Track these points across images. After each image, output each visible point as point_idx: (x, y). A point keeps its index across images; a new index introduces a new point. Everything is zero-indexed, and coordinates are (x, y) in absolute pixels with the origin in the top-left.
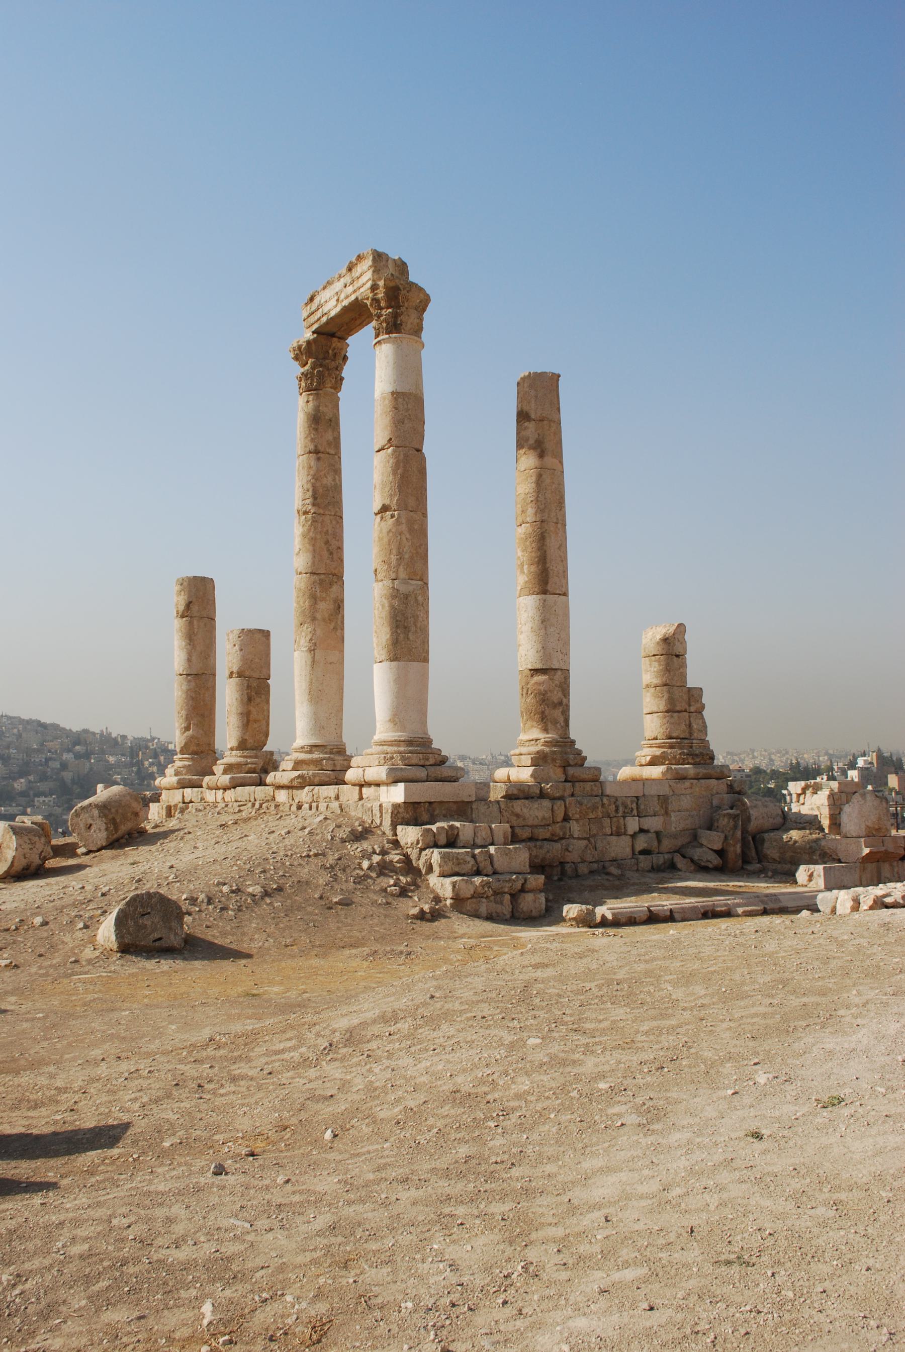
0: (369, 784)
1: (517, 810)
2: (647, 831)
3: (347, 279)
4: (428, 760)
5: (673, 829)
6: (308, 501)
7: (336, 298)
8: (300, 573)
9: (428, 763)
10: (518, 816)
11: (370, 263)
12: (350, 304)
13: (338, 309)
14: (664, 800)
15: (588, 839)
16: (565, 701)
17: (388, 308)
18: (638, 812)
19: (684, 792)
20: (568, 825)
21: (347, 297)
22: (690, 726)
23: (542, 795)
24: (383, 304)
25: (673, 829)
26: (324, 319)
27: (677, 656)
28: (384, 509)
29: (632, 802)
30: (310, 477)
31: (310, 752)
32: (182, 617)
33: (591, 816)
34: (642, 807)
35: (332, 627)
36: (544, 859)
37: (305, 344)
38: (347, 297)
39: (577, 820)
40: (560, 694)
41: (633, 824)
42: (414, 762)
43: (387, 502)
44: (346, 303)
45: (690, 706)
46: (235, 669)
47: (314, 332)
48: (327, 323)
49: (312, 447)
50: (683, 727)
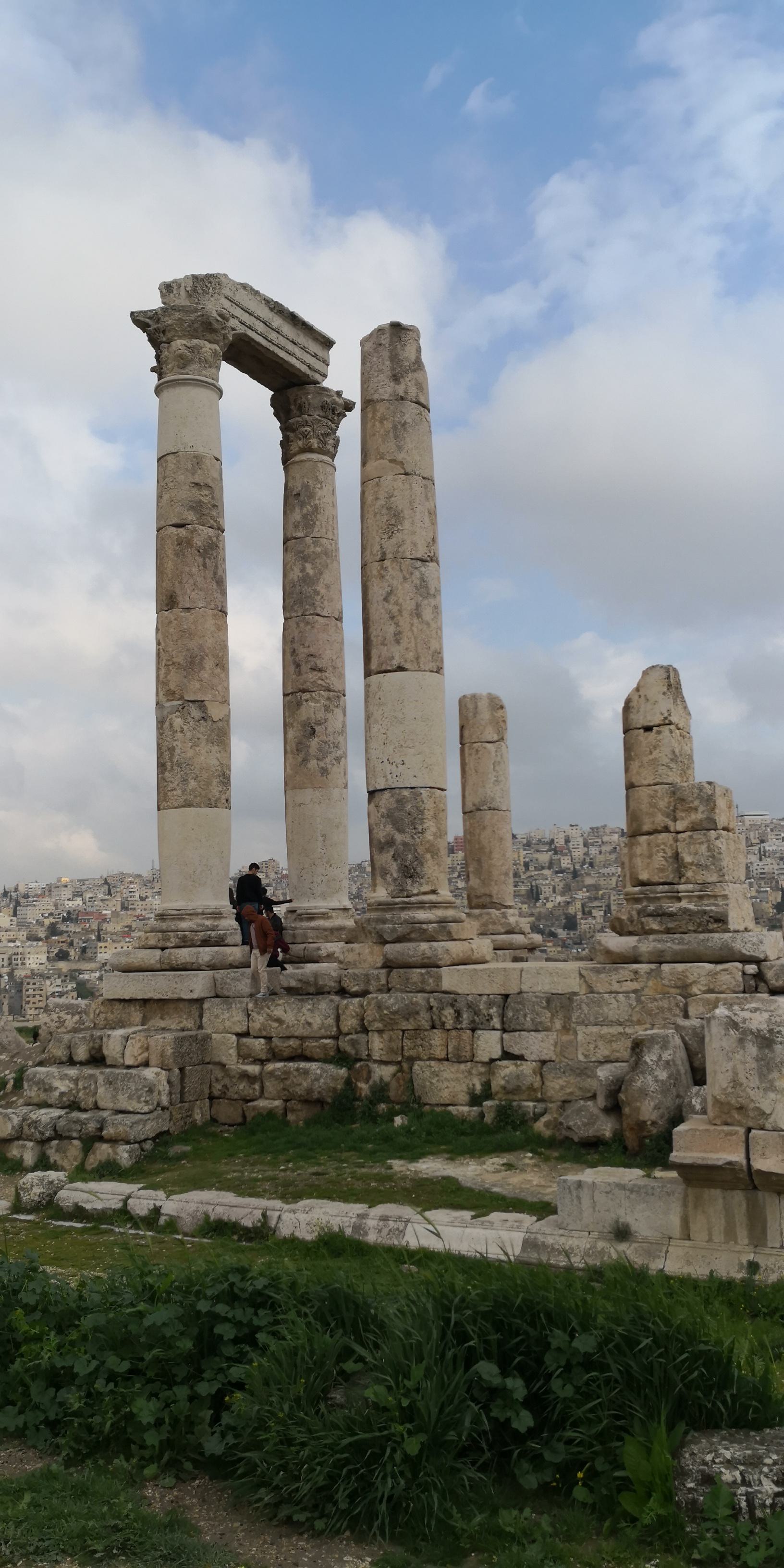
1: (278, 1012)
2: (521, 1058)
4: (169, 939)
5: (581, 1058)
10: (279, 1021)
14: (561, 1003)
15: (399, 1063)
16: (399, 837)
18: (503, 1023)
19: (616, 987)
20: (362, 1037)
22: (677, 856)
23: (342, 992)
25: (581, 1058)
27: (648, 729)
29: (490, 1004)
33: (405, 1025)
34: (510, 1014)
35: (300, 759)
36: (309, 1091)
39: (380, 1032)
40: (389, 828)
41: (489, 1043)
42: (152, 942)
45: (675, 820)
50: (659, 860)
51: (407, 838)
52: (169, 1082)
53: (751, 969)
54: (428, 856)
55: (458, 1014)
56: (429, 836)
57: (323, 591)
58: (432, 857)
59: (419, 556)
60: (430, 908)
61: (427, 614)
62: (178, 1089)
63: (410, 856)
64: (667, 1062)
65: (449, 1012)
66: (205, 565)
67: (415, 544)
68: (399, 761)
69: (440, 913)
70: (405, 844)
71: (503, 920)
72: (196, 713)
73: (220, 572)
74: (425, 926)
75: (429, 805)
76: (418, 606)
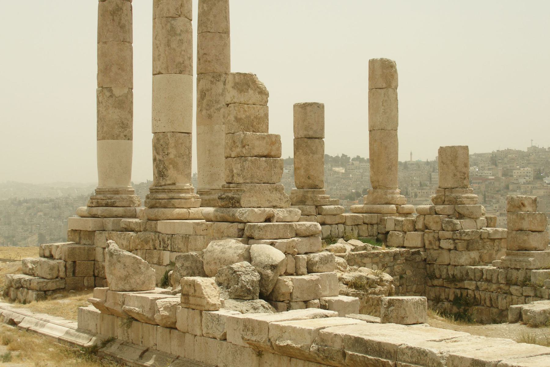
9: (93, 205)
19: (202, 233)
41: (167, 257)
51: (161, 158)
52: (65, 267)
53: (241, 226)
54: (171, 166)
55: (160, 241)
56: (172, 156)
57: (212, 19)
58: (173, 167)
59: (170, 15)
60: (168, 192)
61: (174, 45)
62: (70, 270)
63: (162, 166)
64: (187, 267)
65: (158, 242)
66: (113, 20)
67: (168, 10)
68: (158, 119)
69: (171, 195)
70: (160, 160)
71: (384, 196)
72: (108, 94)
73: (123, 21)
74: (160, 200)
75: (172, 141)
76: (169, 41)
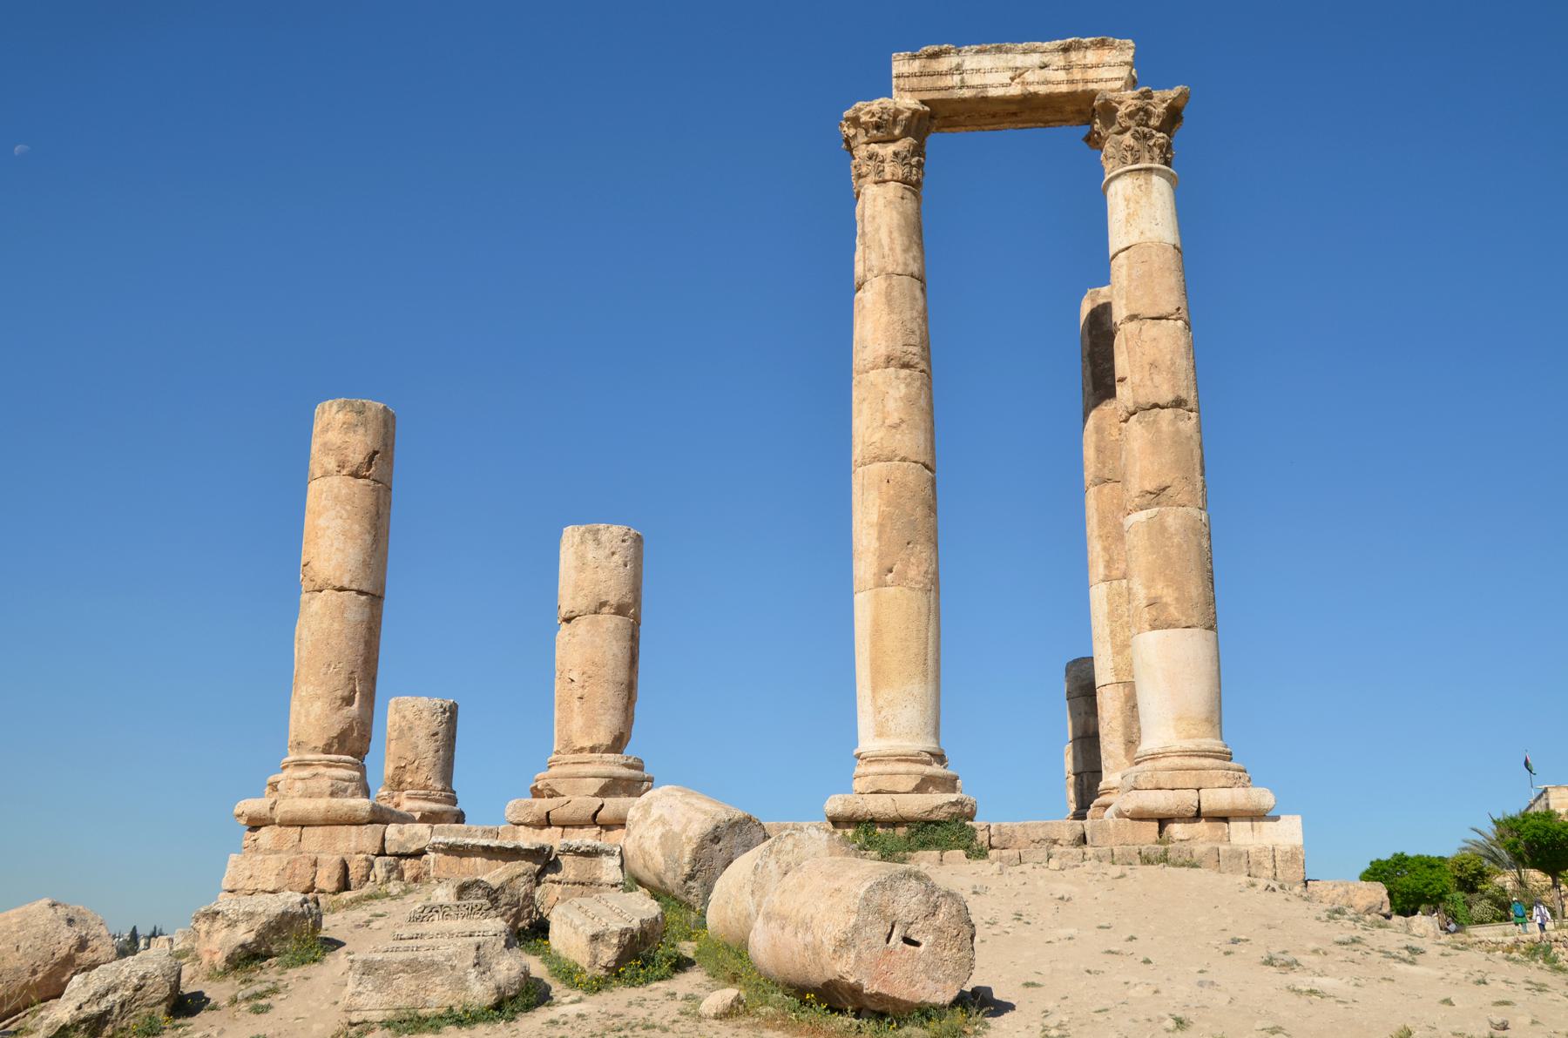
0: (1198, 816)
3: (1058, 60)
6: (910, 349)
7: (1010, 74)
8: (904, 459)
11: (1128, 56)
12: (1049, 96)
13: (1015, 90)
17: (1159, 130)
21: (1046, 82)
24: (1154, 122)
26: (967, 93)
28: (1178, 403)
30: (915, 314)
31: (929, 763)
32: (355, 475)
37: (907, 114)
38: (1046, 82)
43: (1184, 395)
44: (1043, 90)
46: (613, 599)
47: (923, 102)
48: (964, 101)
49: (914, 268)
